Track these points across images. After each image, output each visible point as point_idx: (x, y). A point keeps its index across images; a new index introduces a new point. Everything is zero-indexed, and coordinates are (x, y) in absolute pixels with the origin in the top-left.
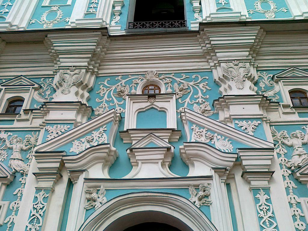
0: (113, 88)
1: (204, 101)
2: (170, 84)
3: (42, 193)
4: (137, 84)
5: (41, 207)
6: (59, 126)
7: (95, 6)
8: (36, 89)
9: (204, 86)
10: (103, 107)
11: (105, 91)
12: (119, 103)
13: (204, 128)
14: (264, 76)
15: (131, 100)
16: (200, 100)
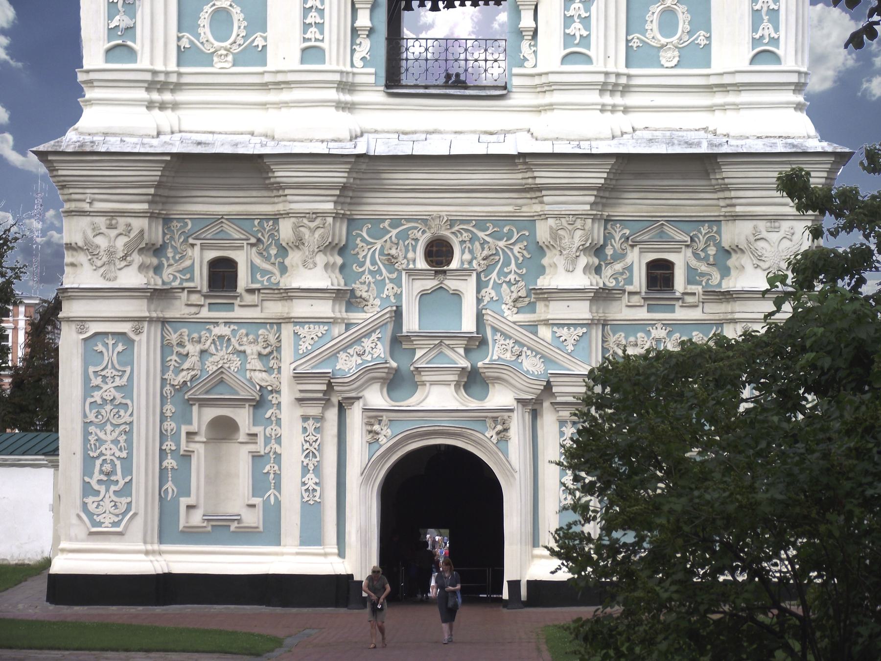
0: (378, 246)
1: (518, 279)
2: (468, 245)
3: (311, 422)
4: (416, 240)
5: (315, 439)
6: (312, 326)
7: (318, 20)
8: (252, 245)
9: (520, 250)
10: (365, 282)
11: (366, 250)
12: (390, 276)
13: (510, 338)
14: (616, 231)
15: (409, 275)
16: (512, 277)
